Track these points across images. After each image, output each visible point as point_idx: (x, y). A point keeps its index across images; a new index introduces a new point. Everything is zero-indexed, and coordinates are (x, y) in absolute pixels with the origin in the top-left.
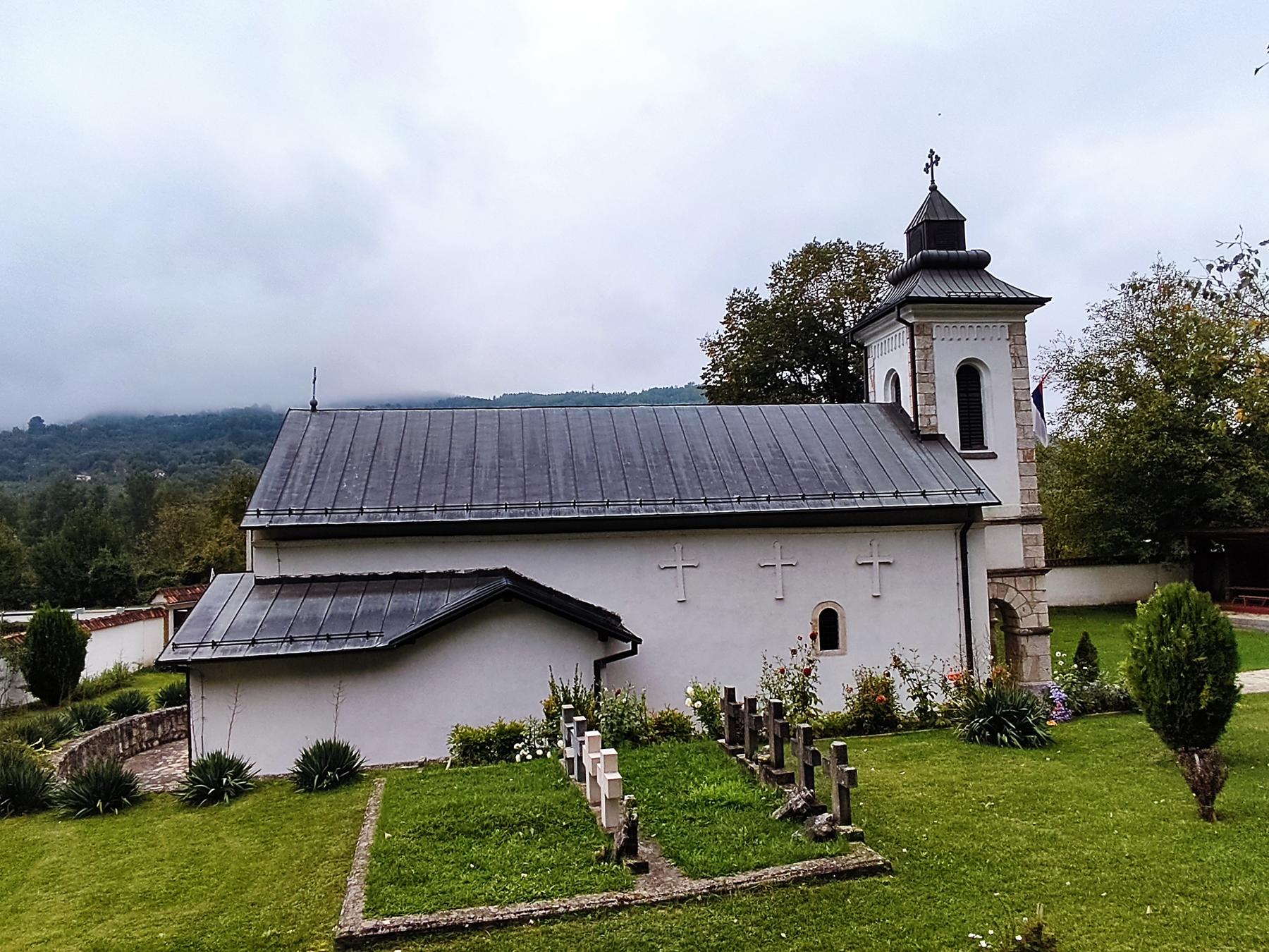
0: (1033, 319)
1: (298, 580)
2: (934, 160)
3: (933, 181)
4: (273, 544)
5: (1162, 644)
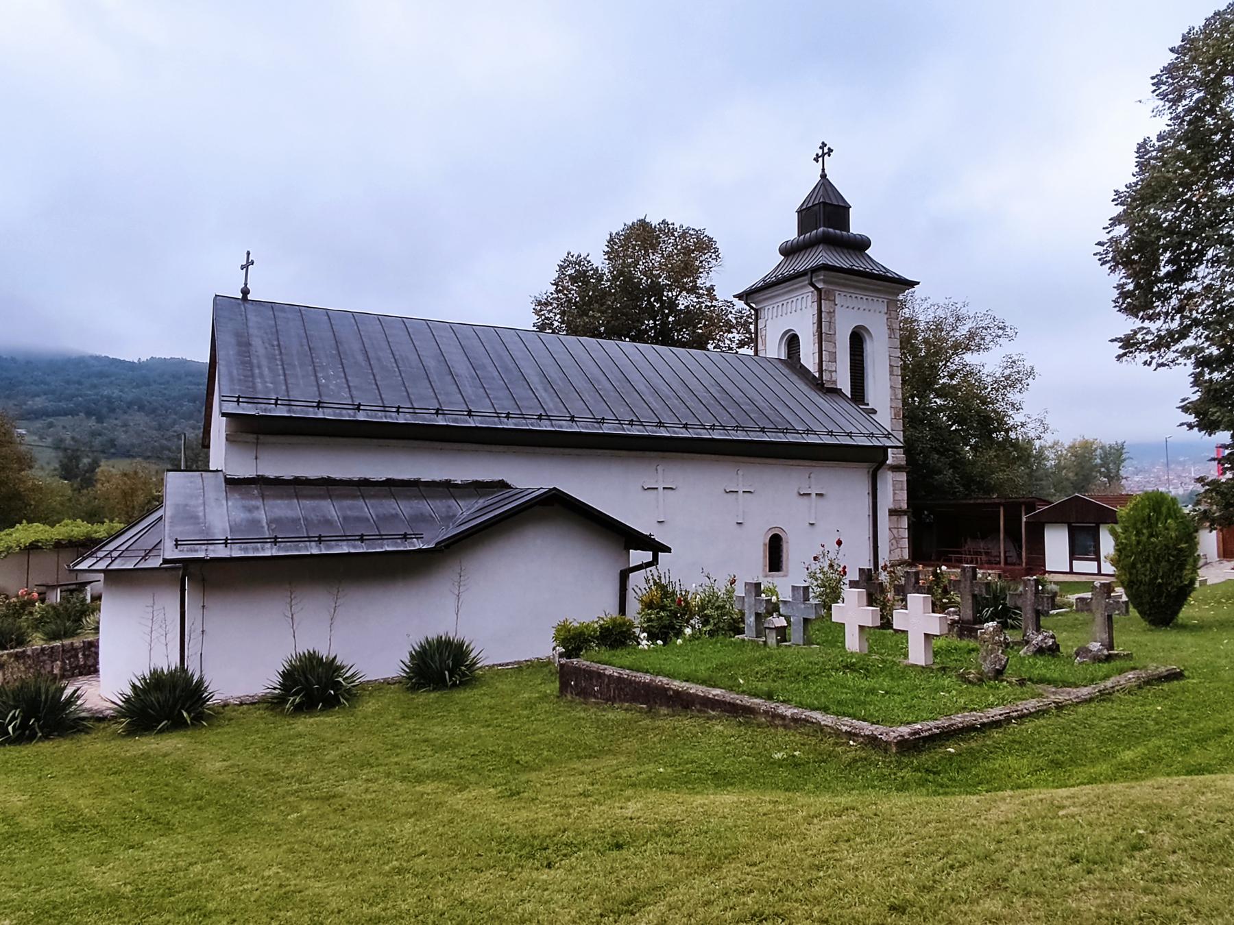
1: (278, 482)
2: (825, 152)
4: (251, 437)
5: (1151, 535)
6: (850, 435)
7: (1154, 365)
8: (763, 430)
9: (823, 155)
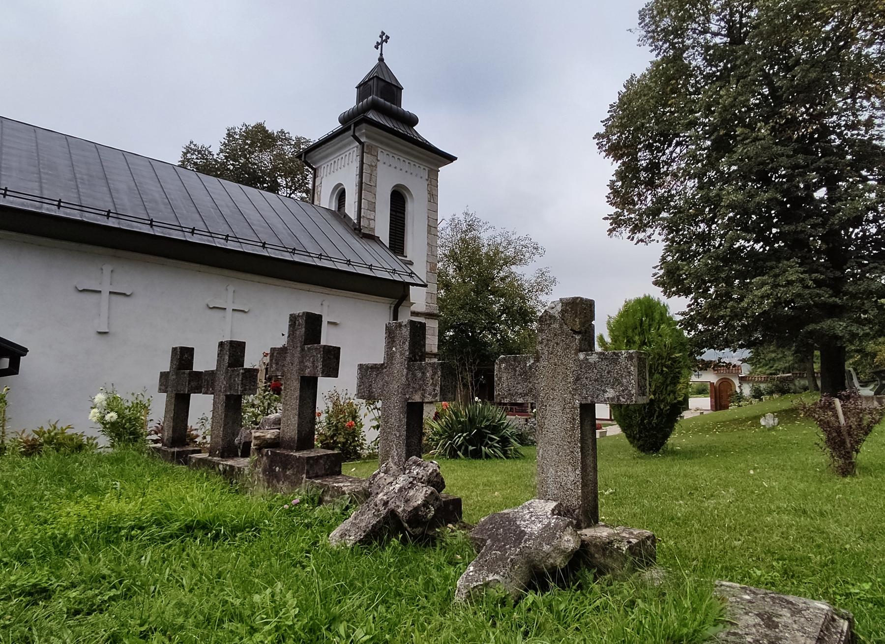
0: (445, 172)
2: (384, 38)
3: (381, 54)
5: (644, 343)
6: (370, 267)
7: (635, 240)
8: (264, 246)
9: (382, 42)
